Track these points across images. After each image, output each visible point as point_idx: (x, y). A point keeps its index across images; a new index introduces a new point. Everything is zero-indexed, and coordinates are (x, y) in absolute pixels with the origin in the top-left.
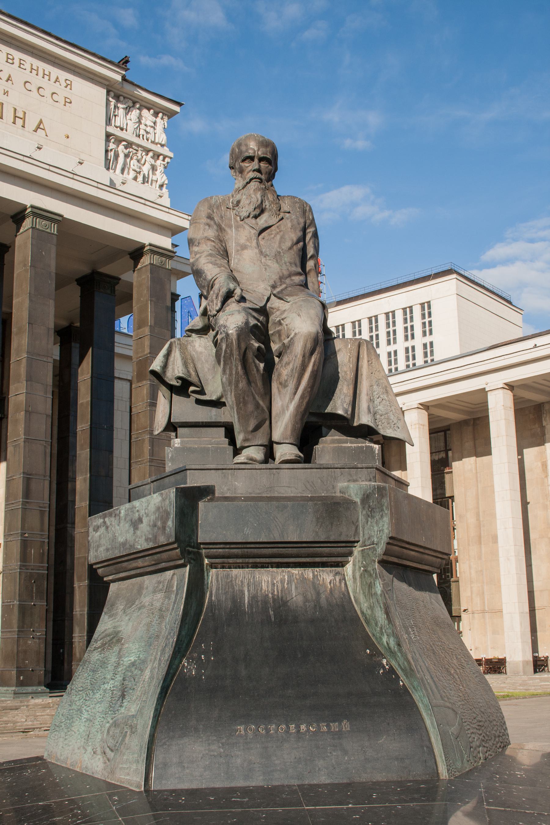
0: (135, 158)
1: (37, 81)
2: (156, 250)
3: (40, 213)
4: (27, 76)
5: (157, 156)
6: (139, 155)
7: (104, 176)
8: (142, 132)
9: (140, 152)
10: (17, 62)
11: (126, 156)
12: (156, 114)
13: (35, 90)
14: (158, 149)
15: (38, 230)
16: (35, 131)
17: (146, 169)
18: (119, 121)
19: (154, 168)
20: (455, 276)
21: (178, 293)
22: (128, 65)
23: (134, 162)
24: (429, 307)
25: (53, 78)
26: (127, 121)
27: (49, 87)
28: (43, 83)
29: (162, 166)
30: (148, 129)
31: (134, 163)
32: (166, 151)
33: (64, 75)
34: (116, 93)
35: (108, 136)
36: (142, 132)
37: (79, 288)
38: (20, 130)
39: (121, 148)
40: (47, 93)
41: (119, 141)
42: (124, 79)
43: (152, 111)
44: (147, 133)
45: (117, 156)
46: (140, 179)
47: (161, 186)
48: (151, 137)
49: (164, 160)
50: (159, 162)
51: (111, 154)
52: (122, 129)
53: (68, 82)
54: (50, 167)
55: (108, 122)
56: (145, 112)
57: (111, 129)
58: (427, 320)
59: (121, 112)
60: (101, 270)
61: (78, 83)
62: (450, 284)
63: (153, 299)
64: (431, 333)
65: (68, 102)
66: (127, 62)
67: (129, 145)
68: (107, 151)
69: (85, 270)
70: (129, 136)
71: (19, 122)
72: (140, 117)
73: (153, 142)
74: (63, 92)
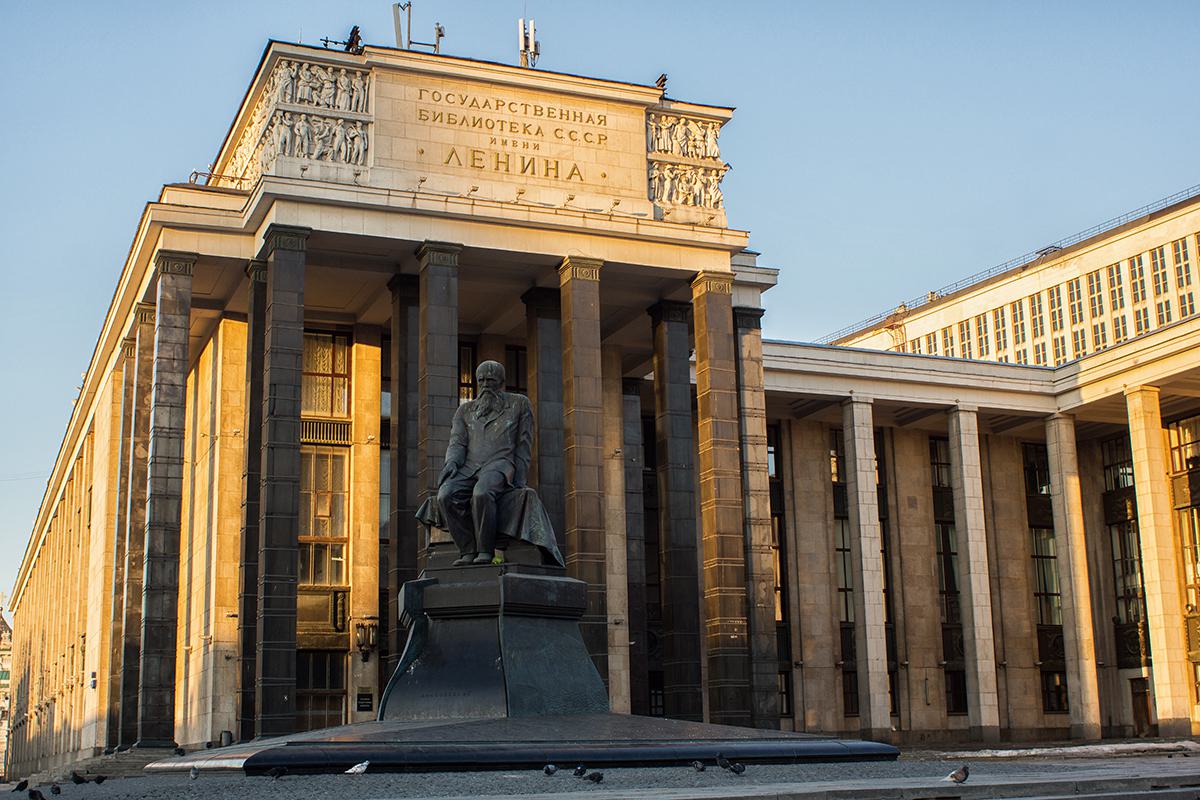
0: (683, 179)
1: (569, 126)
2: (712, 276)
3: (577, 261)
4: (557, 123)
6: (688, 176)
8: (691, 149)
9: (689, 172)
10: (545, 111)
11: (672, 180)
13: (566, 135)
14: (709, 163)
15: (579, 279)
16: (570, 178)
17: (697, 188)
19: (706, 186)
21: (762, 308)
26: (671, 142)
28: (576, 126)
29: (716, 182)
30: (698, 143)
31: (682, 187)
33: (596, 110)
35: (650, 162)
36: (691, 149)
37: (650, 318)
38: (554, 183)
39: (666, 173)
41: (661, 163)
42: (662, 98)
43: (700, 124)
44: (695, 147)
45: (662, 180)
46: (691, 201)
48: (701, 152)
49: (717, 175)
52: (666, 152)
53: (602, 118)
54: (585, 214)
55: (650, 147)
57: (650, 156)
59: (665, 133)
60: (670, 297)
63: (712, 329)
65: (602, 138)
66: (665, 80)
68: (650, 180)
69: (651, 299)
71: (552, 173)
74: (595, 130)
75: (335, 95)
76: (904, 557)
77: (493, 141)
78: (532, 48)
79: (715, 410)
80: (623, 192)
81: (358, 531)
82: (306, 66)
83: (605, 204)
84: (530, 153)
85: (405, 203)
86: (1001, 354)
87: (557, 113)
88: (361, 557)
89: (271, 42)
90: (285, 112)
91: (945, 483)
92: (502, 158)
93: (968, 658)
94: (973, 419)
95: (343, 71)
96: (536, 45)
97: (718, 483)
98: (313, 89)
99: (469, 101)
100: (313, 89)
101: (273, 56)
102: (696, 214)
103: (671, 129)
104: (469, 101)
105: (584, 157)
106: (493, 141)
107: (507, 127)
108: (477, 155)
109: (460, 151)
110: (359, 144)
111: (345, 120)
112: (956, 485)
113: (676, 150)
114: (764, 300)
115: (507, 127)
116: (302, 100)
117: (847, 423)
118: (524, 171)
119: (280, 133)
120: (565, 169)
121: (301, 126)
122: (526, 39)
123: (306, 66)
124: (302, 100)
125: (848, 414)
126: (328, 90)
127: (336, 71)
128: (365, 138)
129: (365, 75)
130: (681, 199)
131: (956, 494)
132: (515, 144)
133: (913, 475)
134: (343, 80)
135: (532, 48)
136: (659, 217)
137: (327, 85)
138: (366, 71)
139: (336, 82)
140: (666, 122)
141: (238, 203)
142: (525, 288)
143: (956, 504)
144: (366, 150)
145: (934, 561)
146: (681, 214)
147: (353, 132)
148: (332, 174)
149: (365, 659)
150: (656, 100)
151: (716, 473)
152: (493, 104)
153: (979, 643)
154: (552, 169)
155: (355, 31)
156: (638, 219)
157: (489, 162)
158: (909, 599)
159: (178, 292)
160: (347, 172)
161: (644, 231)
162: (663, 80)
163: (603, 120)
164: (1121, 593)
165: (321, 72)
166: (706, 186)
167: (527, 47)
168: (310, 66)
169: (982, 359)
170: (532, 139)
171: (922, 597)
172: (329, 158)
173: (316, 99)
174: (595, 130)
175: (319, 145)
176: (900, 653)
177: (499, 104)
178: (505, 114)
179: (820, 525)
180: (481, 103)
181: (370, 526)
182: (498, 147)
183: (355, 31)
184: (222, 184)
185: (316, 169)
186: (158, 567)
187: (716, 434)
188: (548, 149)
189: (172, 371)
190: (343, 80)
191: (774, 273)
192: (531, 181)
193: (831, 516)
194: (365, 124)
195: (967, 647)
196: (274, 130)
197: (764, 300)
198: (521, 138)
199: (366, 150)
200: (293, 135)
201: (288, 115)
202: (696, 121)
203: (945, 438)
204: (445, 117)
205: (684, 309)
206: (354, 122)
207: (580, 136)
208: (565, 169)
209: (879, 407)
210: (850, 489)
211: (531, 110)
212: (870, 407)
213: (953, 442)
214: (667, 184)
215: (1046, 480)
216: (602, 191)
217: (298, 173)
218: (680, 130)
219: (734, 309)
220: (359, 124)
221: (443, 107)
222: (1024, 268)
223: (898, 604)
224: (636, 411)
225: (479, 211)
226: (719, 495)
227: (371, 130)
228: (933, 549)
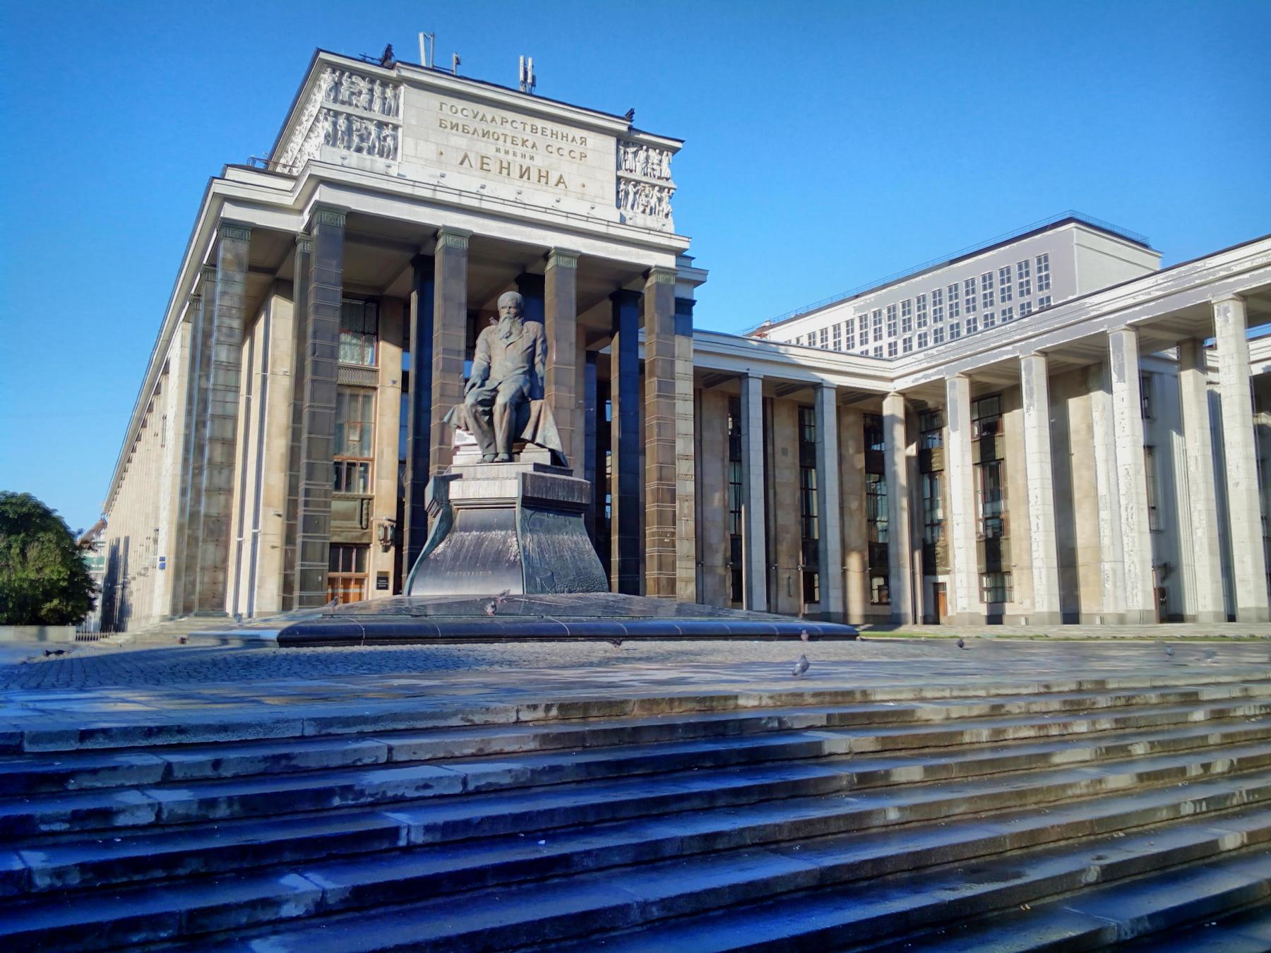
1: (556, 143)
2: (662, 270)
3: (561, 252)
5: (662, 189)
10: (540, 131)
12: (661, 153)
17: (653, 201)
18: (629, 164)
19: (660, 200)
23: (643, 197)
25: (570, 138)
26: (636, 162)
27: (567, 146)
28: (563, 144)
31: (642, 200)
32: (671, 184)
34: (624, 140)
35: (619, 179)
40: (566, 153)
41: (628, 181)
42: (630, 128)
45: (627, 194)
46: (648, 211)
47: (667, 215)
48: (657, 174)
50: (665, 194)
51: (622, 194)
54: (568, 215)
55: (619, 167)
56: (651, 151)
57: (620, 173)
59: (630, 156)
61: (593, 139)
65: (583, 156)
67: (638, 183)
68: (618, 193)
69: (611, 289)
70: (637, 176)
71: (543, 180)
72: (647, 158)
73: (659, 178)
74: (578, 149)
76: (778, 490)
78: (529, 80)
79: (658, 371)
80: (597, 200)
81: (381, 453)
83: (583, 209)
84: (526, 163)
85: (427, 194)
86: (864, 348)
87: (549, 133)
88: (384, 473)
90: (329, 110)
91: (807, 436)
92: (505, 165)
93: (822, 563)
94: (833, 393)
96: (534, 78)
97: (659, 425)
98: (353, 93)
99: (480, 117)
102: (651, 221)
103: (635, 154)
104: (480, 117)
105: (565, 167)
106: (498, 150)
107: (509, 140)
108: (485, 160)
109: (472, 156)
112: (818, 440)
113: (638, 170)
114: (697, 293)
115: (509, 140)
117: (744, 391)
118: (521, 177)
119: (325, 126)
120: (553, 179)
122: (526, 73)
124: (343, 103)
125: (744, 385)
127: (372, 82)
128: (395, 138)
129: (396, 87)
130: (641, 208)
131: (818, 447)
132: (515, 154)
133: (786, 432)
134: (377, 89)
135: (529, 80)
136: (623, 221)
138: (396, 83)
140: (631, 150)
141: (288, 185)
142: (517, 273)
143: (818, 454)
144: (396, 149)
145: (798, 494)
146: (641, 220)
148: (368, 165)
150: (625, 128)
151: (658, 418)
152: (499, 121)
153: (830, 553)
154: (543, 177)
155: (389, 49)
156: (609, 223)
157: (494, 167)
158: (781, 521)
159: (237, 256)
161: (613, 231)
162: (631, 113)
163: (584, 141)
164: (928, 522)
166: (660, 200)
167: (526, 79)
169: (850, 351)
170: (529, 151)
171: (788, 519)
172: (365, 152)
174: (578, 149)
175: (356, 139)
176: (772, 557)
177: (504, 121)
178: (508, 129)
179: (719, 465)
180: (489, 119)
181: (391, 449)
182: (502, 155)
183: (389, 49)
184: (279, 170)
185: (354, 158)
186: (215, 473)
187: (659, 390)
188: (540, 161)
189: (230, 317)
191: (704, 273)
192: (527, 185)
193: (727, 459)
194: (396, 128)
195: (821, 556)
196: (320, 125)
197: (697, 293)
198: (520, 149)
203: (811, 407)
204: (460, 128)
205: (636, 298)
207: (566, 153)
208: (553, 179)
209: (767, 382)
210: (744, 439)
211: (528, 128)
212: (760, 382)
213: (817, 409)
214: (631, 197)
215: (880, 440)
216: (582, 197)
217: (339, 162)
218: (642, 154)
219: (677, 299)
221: (459, 119)
223: (772, 524)
224: (593, 376)
225: (486, 205)
226: (659, 434)
227: (400, 130)
228: (798, 485)
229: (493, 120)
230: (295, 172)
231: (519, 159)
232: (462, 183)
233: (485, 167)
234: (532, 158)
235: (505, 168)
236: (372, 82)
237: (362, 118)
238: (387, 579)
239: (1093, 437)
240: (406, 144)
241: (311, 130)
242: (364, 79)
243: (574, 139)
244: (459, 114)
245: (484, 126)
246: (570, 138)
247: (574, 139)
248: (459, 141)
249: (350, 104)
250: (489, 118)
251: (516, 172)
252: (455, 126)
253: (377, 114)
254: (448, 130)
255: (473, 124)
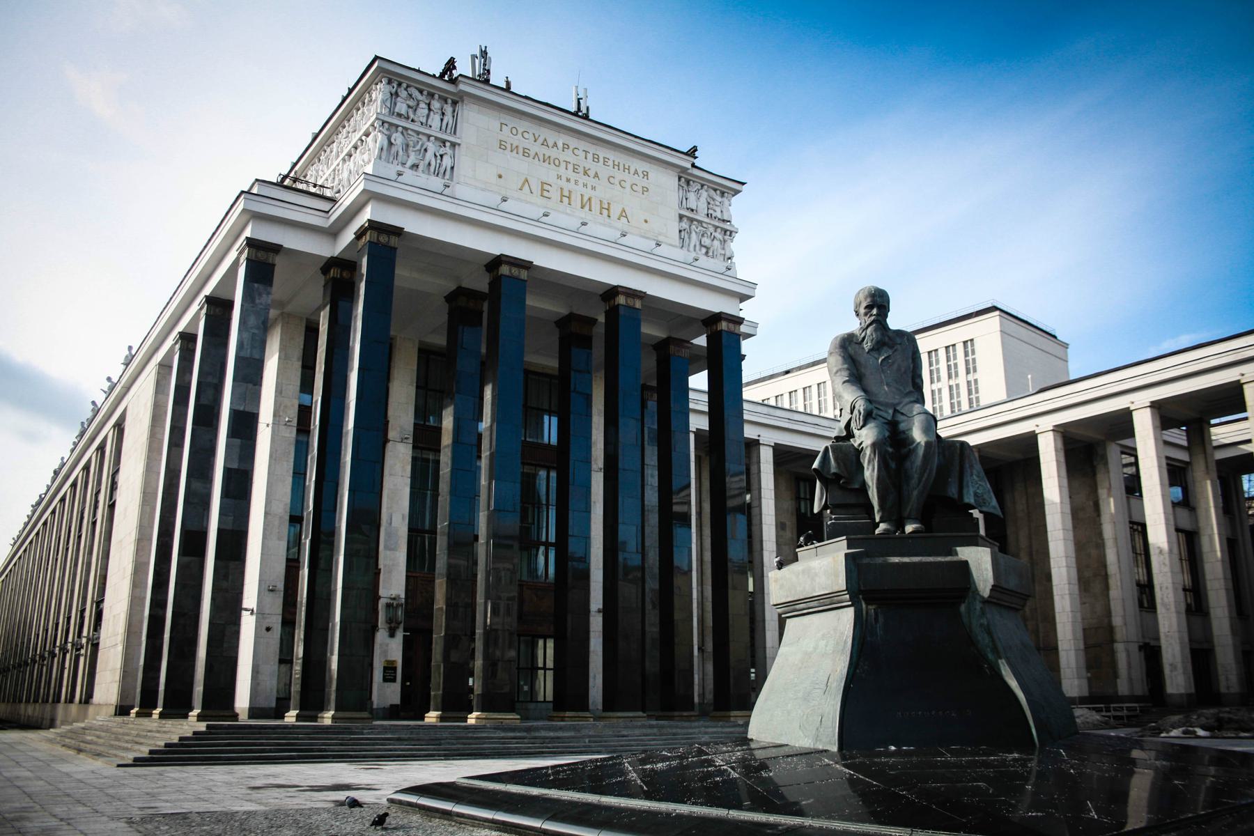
1: (619, 175)
4: (609, 171)
7: (679, 254)
10: (601, 160)
20: (997, 313)
22: (697, 154)
24: (972, 345)
25: (632, 171)
27: (629, 179)
28: (625, 176)
33: (640, 166)
38: (607, 220)
40: (628, 185)
56: (712, 192)
58: (970, 358)
62: (994, 320)
64: (975, 371)
65: (645, 190)
71: (605, 212)
75: (428, 116)
77: (559, 177)
82: (404, 85)
84: (588, 193)
89: (376, 58)
95: (436, 96)
99: (541, 140)
100: (409, 107)
101: (385, 72)
107: (570, 167)
108: (546, 187)
110: (447, 162)
111: (436, 138)
116: (399, 115)
121: (398, 138)
123: (404, 85)
126: (423, 110)
127: (431, 95)
129: (455, 103)
132: (576, 182)
134: (436, 105)
137: (422, 105)
139: (429, 105)
141: (325, 206)
144: (452, 168)
147: (442, 151)
149: (392, 635)
152: (560, 145)
160: (436, 183)
162: (695, 149)
163: (646, 175)
165: (416, 93)
168: (408, 86)
170: (591, 181)
172: (421, 168)
173: (412, 116)
177: (566, 147)
180: (551, 144)
182: (563, 183)
185: (409, 176)
188: (603, 192)
190: (436, 105)
191: (755, 325)
194: (454, 145)
199: (452, 168)
200: (391, 144)
201: (386, 125)
202: (715, 190)
206: (444, 142)
207: (628, 185)
208: (615, 211)
211: (590, 156)
217: (394, 176)
218: (704, 194)
220: (448, 144)
222: (787, 372)
229: (555, 145)
230: (328, 193)
231: (580, 187)
232: (525, 209)
233: (545, 193)
234: (593, 188)
235: (566, 197)
236: (431, 95)
237: (418, 133)
238: (395, 669)
239: (1099, 515)
240: (465, 163)
241: (356, 148)
242: (421, 92)
243: (636, 172)
244: (520, 135)
245: (548, 152)
246: (632, 171)
247: (636, 172)
248: (519, 165)
249: (408, 118)
250: (551, 144)
251: (577, 202)
252: (515, 149)
253: (435, 132)
254: (508, 152)
255: (535, 148)
